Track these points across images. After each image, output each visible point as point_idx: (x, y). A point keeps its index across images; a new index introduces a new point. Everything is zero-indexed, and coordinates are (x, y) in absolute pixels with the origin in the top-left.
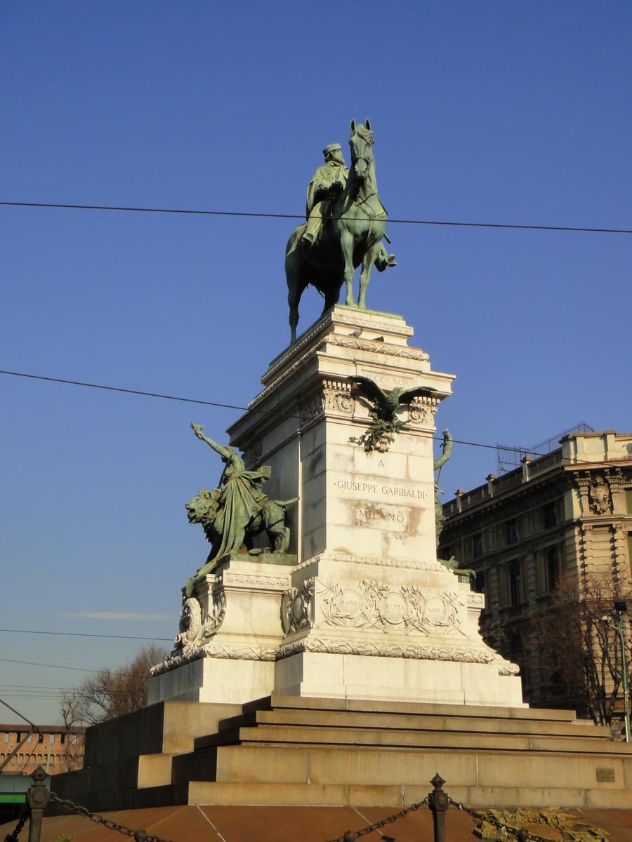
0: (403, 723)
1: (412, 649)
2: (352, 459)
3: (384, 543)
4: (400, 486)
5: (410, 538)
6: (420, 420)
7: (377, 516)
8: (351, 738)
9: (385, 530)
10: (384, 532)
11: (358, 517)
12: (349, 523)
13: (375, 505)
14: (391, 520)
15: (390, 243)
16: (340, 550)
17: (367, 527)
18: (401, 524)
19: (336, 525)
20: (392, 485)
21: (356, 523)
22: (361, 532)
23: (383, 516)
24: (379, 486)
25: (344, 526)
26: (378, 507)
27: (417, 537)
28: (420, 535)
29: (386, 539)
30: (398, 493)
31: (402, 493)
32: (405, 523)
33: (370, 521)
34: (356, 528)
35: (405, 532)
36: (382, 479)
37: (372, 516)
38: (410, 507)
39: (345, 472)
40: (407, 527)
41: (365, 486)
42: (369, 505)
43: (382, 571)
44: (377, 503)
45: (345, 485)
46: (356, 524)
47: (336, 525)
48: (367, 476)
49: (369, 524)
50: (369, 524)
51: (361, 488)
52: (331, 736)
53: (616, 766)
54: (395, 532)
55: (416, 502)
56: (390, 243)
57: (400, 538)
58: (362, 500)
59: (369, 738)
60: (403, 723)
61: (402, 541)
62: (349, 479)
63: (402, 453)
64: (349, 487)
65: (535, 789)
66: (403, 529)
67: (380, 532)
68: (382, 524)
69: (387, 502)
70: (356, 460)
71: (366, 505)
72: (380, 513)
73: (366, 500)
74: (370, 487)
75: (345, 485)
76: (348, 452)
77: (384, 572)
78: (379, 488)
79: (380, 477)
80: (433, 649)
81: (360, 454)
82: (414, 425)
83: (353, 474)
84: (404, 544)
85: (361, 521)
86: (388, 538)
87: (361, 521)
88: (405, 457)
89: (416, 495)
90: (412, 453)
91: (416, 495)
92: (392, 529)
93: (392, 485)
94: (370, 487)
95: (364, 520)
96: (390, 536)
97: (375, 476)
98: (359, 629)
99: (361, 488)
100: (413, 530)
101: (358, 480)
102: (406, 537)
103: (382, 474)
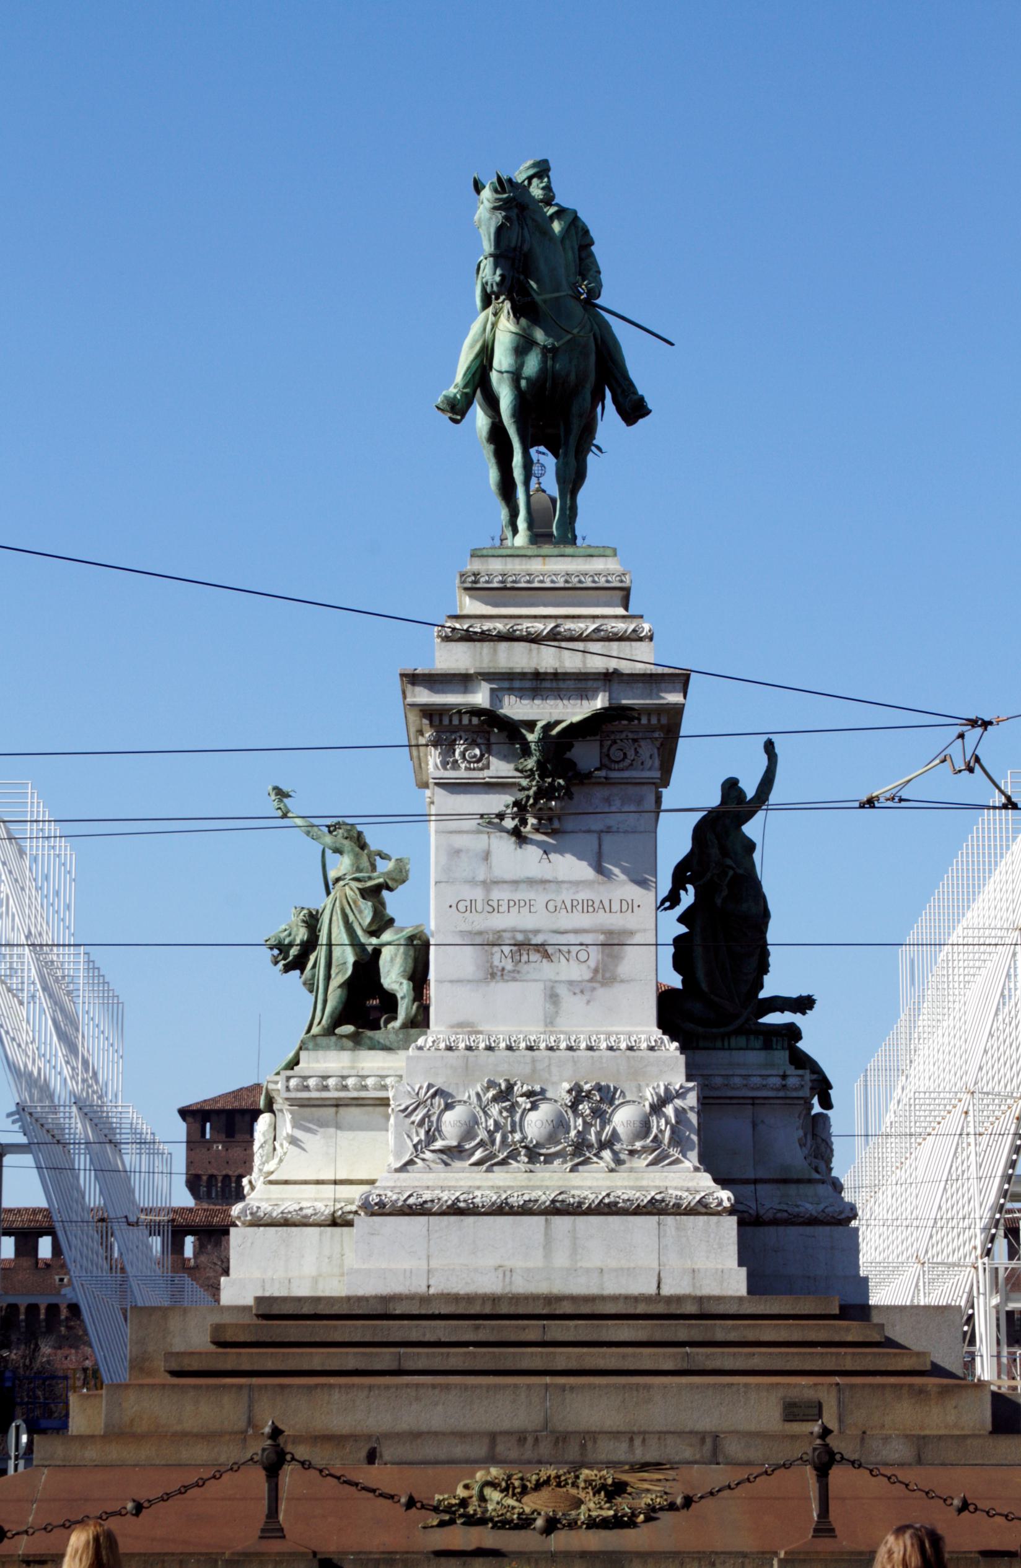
0: (465, 1331)
1: (560, 1198)
2: (487, 856)
3: (548, 1006)
4: (582, 895)
5: (601, 992)
6: (627, 762)
7: (535, 957)
8: (351, 1359)
9: (550, 981)
10: (549, 984)
11: (496, 963)
12: (481, 975)
13: (531, 936)
14: (562, 957)
15: (672, 344)
16: (460, 1025)
17: (514, 980)
18: (584, 967)
19: (451, 981)
20: (567, 896)
21: (493, 974)
22: (503, 991)
23: (547, 956)
24: (539, 898)
25: (469, 981)
26: (538, 939)
27: (616, 985)
28: (622, 981)
29: (553, 997)
30: (580, 907)
31: (589, 906)
32: (592, 963)
33: (524, 968)
34: (493, 984)
35: (591, 980)
36: (547, 886)
37: (524, 958)
38: (603, 933)
39: (472, 882)
40: (596, 971)
41: (512, 903)
42: (520, 937)
43: (528, 1060)
44: (536, 932)
45: (472, 906)
46: (493, 975)
47: (451, 981)
48: (516, 883)
49: (519, 972)
50: (519, 972)
51: (504, 908)
52: (317, 1359)
53: (823, 1391)
54: (571, 983)
55: (615, 921)
56: (672, 344)
57: (582, 992)
58: (504, 931)
59: (385, 1358)
60: (465, 1331)
61: (585, 998)
62: (478, 894)
63: (589, 831)
64: (479, 909)
65: (616, 1435)
66: (588, 975)
67: (541, 985)
68: (546, 970)
69: (555, 927)
70: (494, 859)
71: (514, 938)
72: (542, 950)
73: (514, 930)
74: (522, 903)
75: (472, 906)
76: (481, 842)
77: (534, 1061)
78: (539, 905)
79: (544, 882)
80: (608, 1195)
81: (503, 846)
82: (614, 775)
83: (489, 884)
84: (588, 1002)
85: (503, 969)
86: (557, 996)
87: (503, 969)
88: (596, 835)
89: (616, 907)
90: (609, 827)
91: (616, 907)
92: (563, 977)
93: (567, 896)
94: (522, 903)
95: (509, 966)
96: (562, 990)
97: (531, 882)
98: (475, 1168)
99: (504, 908)
100: (608, 975)
101: (496, 894)
102: (593, 989)
103: (548, 877)
